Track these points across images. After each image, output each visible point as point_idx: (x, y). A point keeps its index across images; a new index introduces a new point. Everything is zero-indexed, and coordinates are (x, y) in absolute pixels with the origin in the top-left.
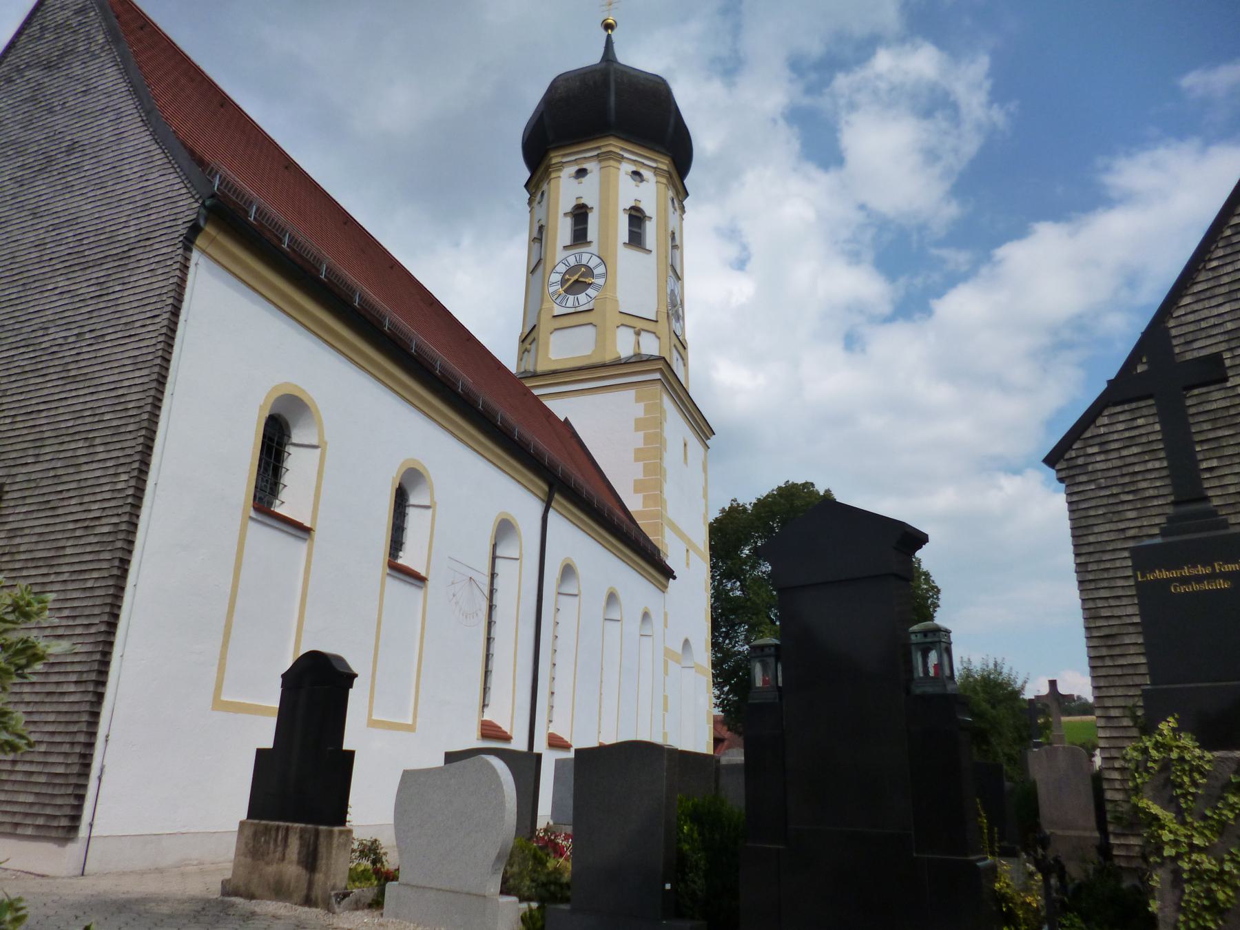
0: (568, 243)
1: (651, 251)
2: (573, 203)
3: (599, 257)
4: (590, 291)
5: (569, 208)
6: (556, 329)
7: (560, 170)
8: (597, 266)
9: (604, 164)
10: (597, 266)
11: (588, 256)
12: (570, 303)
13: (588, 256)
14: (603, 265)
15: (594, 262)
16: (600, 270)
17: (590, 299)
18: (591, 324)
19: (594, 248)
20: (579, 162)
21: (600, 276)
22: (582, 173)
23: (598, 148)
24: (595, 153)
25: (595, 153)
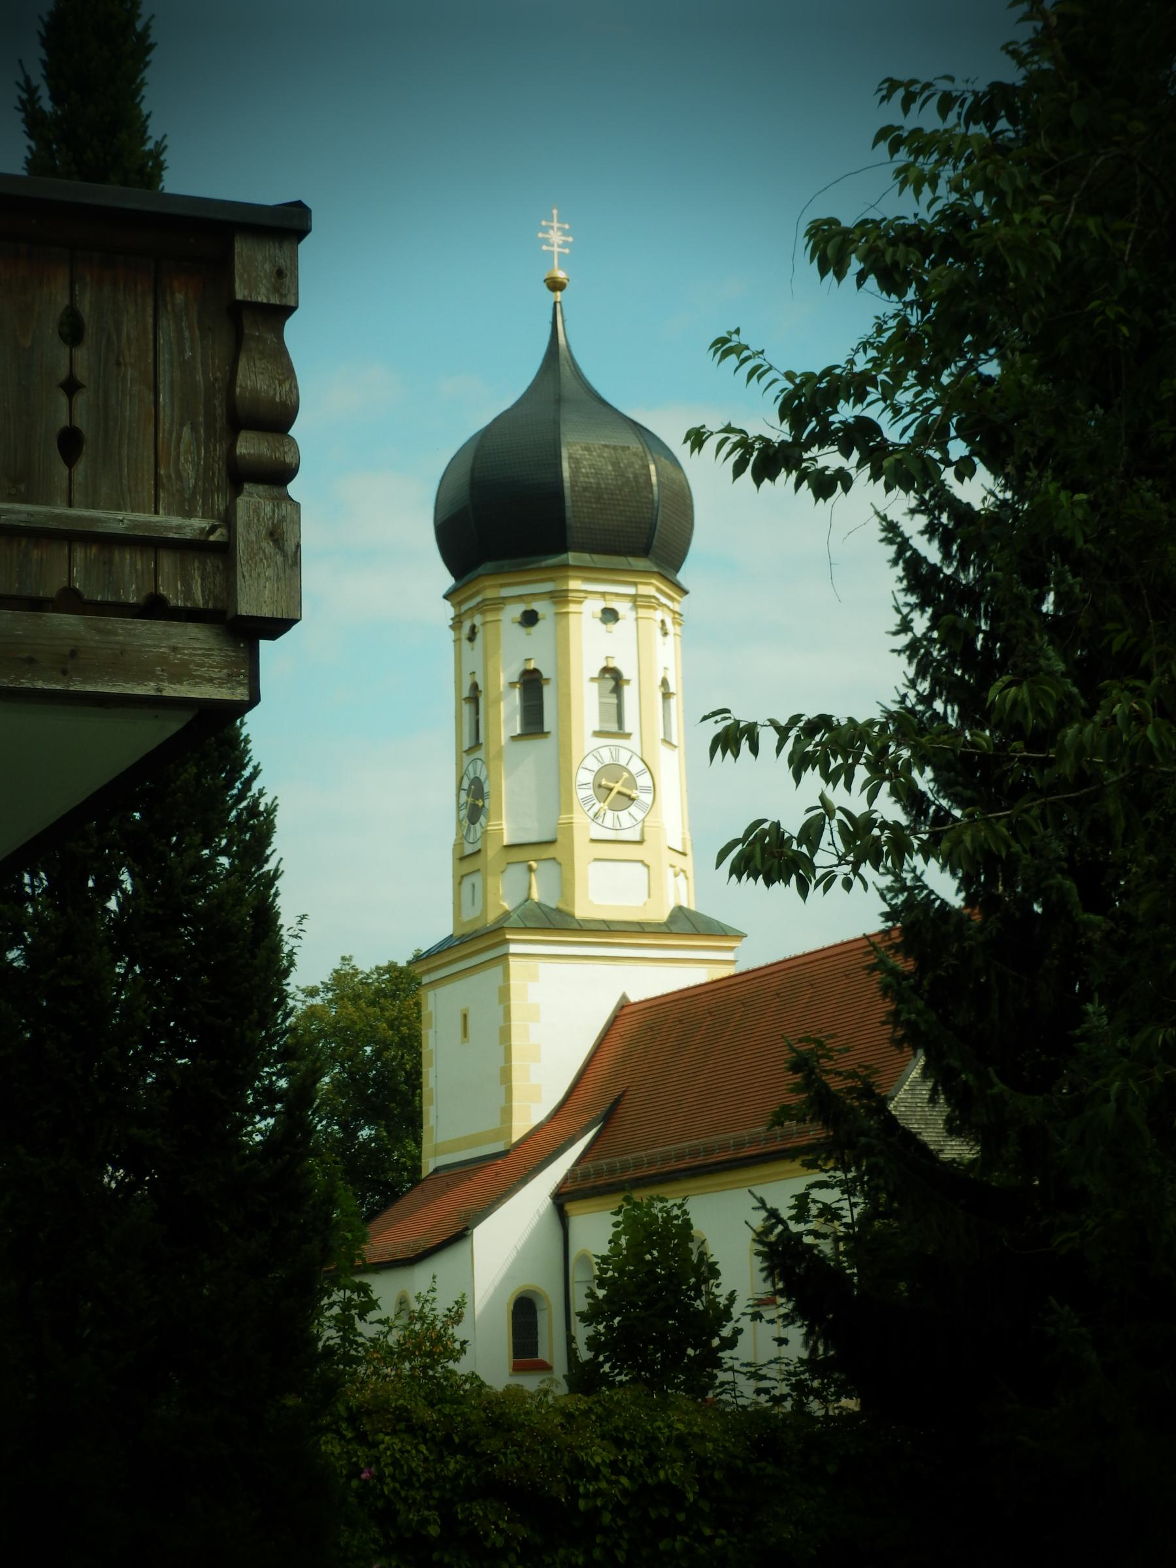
0: (597, 729)
1: (676, 747)
2: (603, 664)
3: (643, 760)
4: (633, 809)
5: (596, 674)
6: (596, 860)
7: (581, 602)
8: (640, 773)
9: (642, 613)
10: (640, 773)
11: (625, 753)
12: (608, 822)
13: (625, 753)
14: (648, 774)
15: (636, 766)
16: (644, 780)
17: (635, 823)
18: (642, 862)
19: (633, 743)
20: (608, 597)
21: (645, 790)
22: (610, 615)
23: (635, 584)
24: (631, 590)
25: (631, 590)
